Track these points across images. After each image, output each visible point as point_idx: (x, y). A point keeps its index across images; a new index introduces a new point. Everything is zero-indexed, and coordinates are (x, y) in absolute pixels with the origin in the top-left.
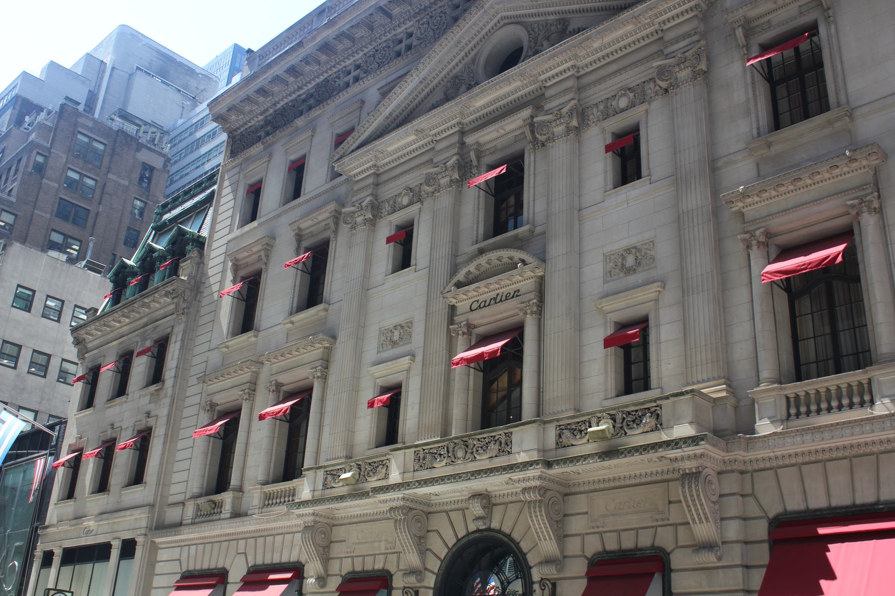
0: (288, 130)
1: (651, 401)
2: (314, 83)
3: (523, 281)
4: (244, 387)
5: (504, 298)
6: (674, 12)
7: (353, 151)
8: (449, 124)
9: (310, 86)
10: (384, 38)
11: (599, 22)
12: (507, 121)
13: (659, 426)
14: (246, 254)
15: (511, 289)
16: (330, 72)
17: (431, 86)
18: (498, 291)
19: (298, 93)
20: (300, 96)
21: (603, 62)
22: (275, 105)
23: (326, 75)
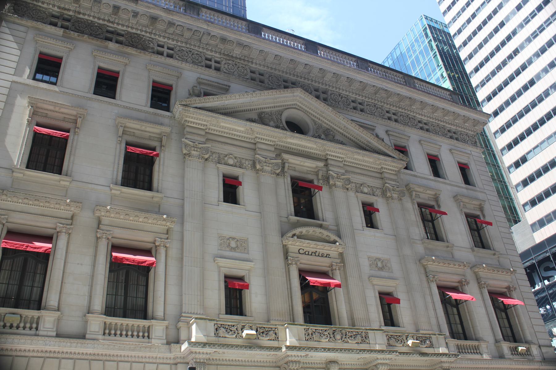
0: (98, 42)
1: (428, 334)
2: (125, 28)
3: (333, 250)
4: (63, 221)
5: (320, 255)
6: (391, 168)
7: (196, 108)
8: (270, 139)
9: (120, 27)
10: (196, 48)
11: (351, 146)
12: (309, 161)
13: (431, 346)
14: (51, 108)
15: (326, 252)
16: (143, 33)
17: (252, 107)
18: (317, 250)
19: (106, 23)
20: (108, 26)
21: (353, 165)
22: (79, 13)
23: (139, 32)
